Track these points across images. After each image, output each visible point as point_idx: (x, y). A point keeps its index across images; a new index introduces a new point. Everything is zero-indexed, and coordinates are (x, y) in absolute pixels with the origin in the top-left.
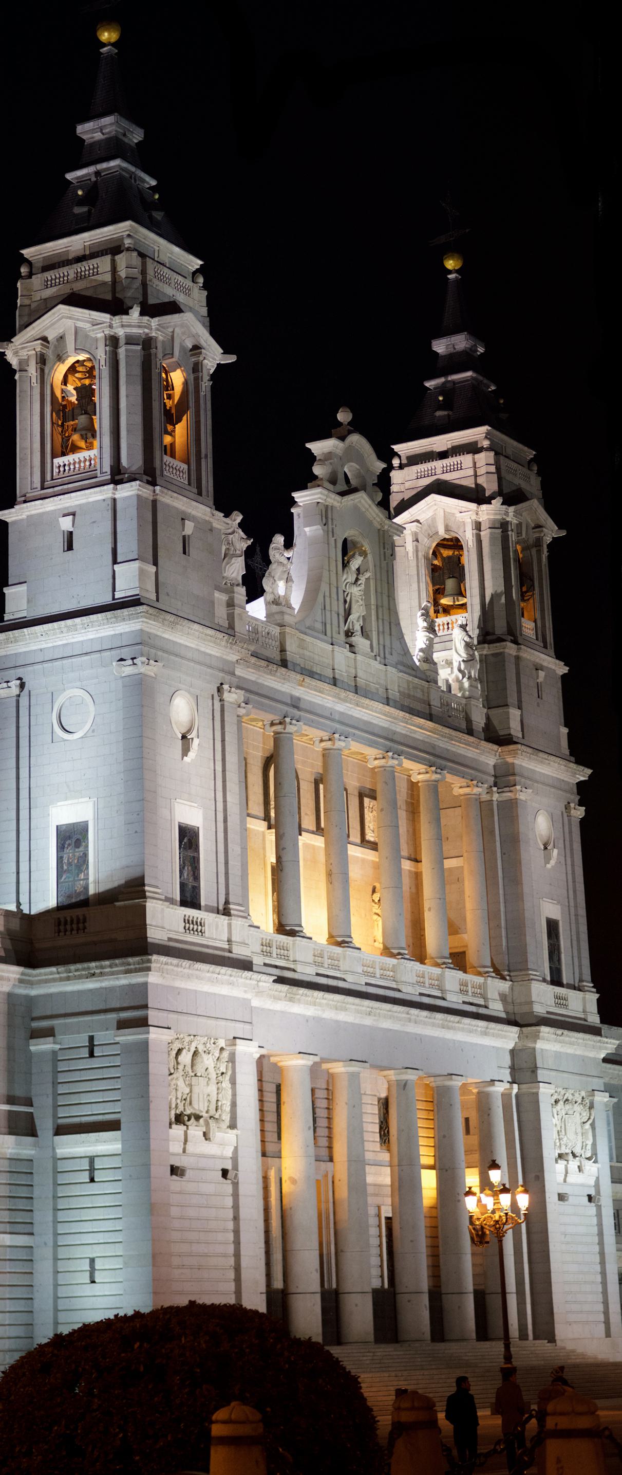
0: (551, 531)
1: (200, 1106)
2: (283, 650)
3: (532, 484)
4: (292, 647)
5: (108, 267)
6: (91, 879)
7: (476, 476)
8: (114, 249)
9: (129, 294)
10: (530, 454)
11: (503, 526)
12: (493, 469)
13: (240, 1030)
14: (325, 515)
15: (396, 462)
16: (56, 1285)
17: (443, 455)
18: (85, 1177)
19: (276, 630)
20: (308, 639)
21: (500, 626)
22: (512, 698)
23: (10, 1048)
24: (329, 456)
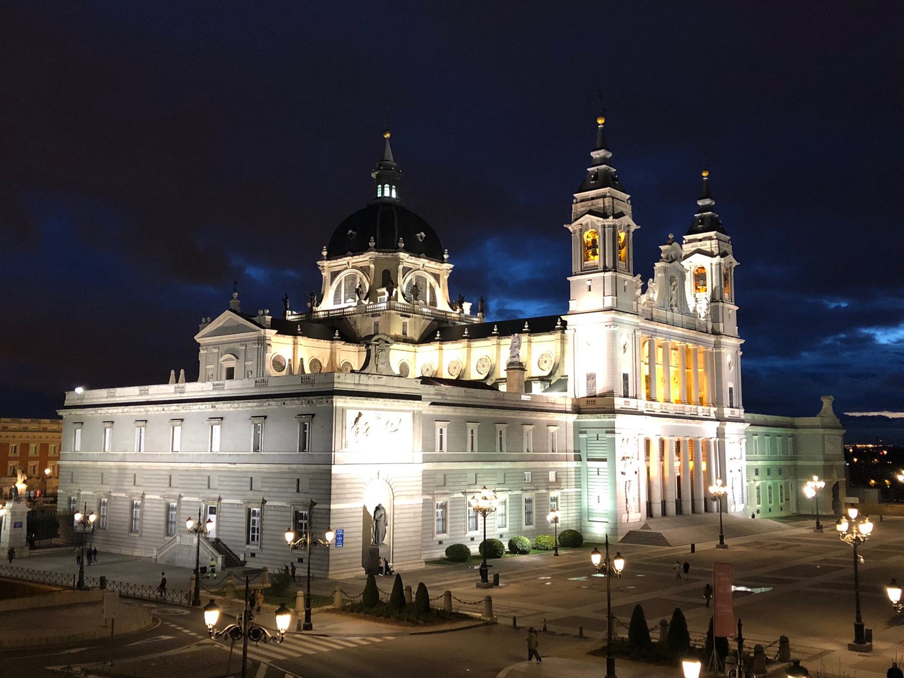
0: (735, 263)
2: (652, 315)
3: (729, 248)
4: (654, 314)
5: (602, 202)
8: (604, 196)
9: (609, 211)
10: (729, 238)
11: (720, 264)
12: (717, 245)
14: (665, 270)
15: (684, 242)
17: (700, 240)
18: (596, 473)
19: (650, 309)
20: (660, 310)
22: (721, 320)
23: (574, 437)
24: (666, 250)
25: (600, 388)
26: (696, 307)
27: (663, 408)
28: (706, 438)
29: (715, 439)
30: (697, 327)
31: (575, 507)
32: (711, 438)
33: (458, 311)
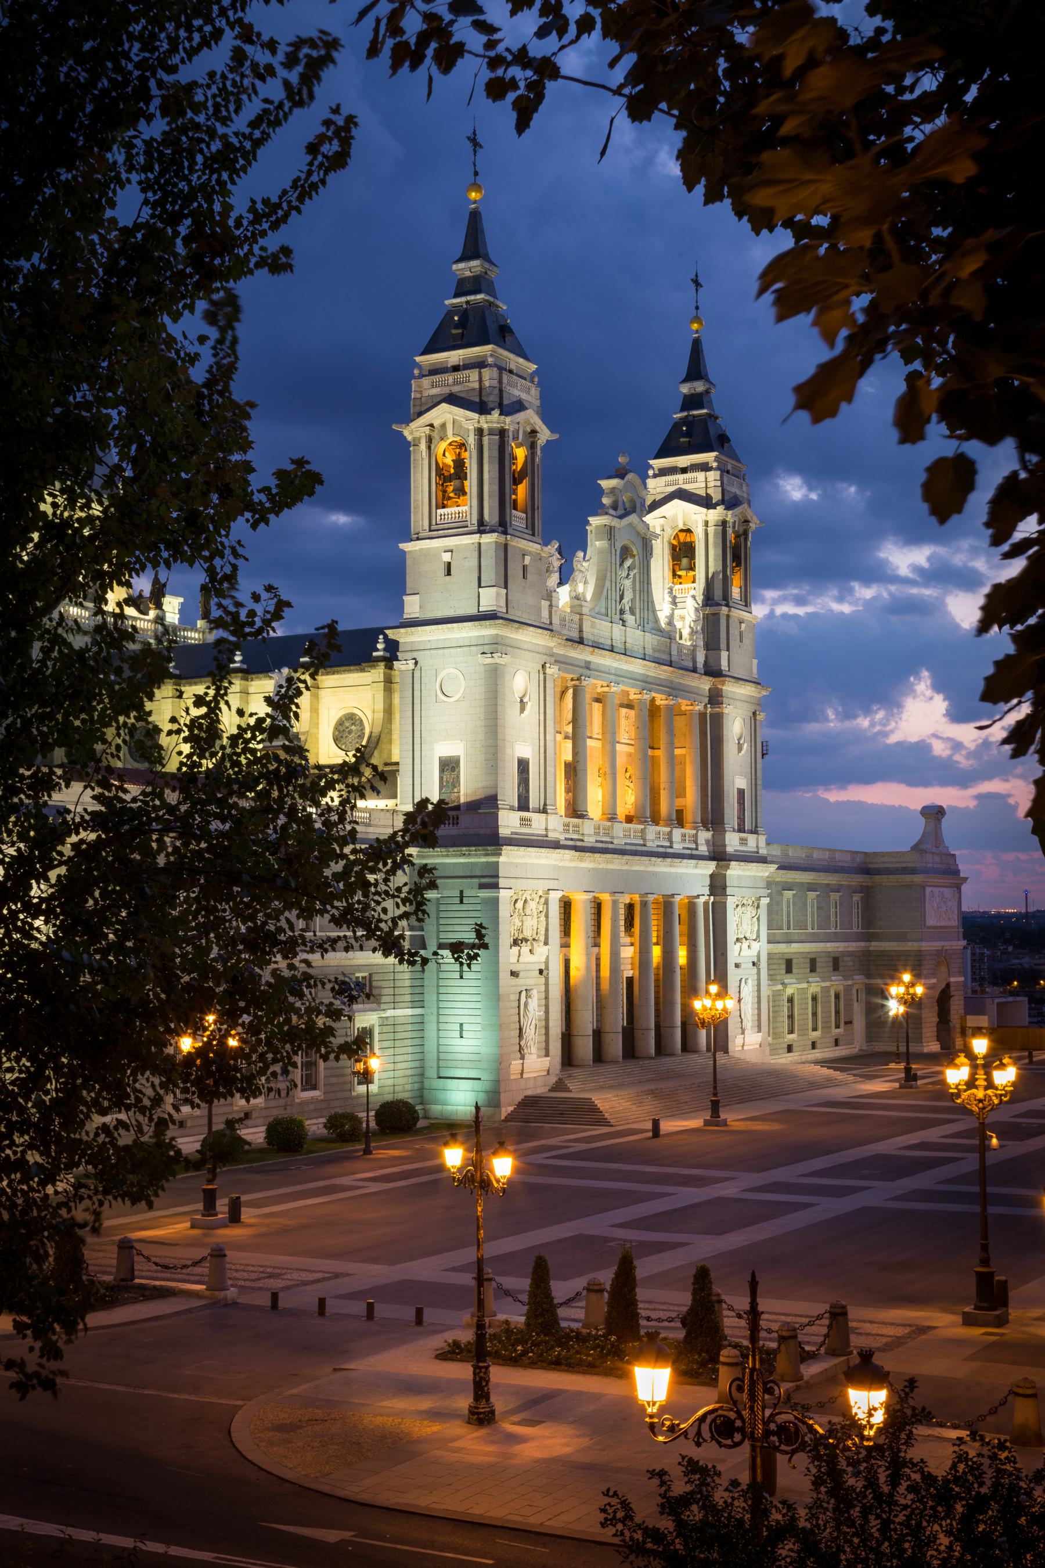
1: (528, 933)
2: (581, 631)
5: (477, 379)
6: (462, 792)
7: (706, 487)
8: (480, 364)
11: (724, 523)
12: (719, 483)
13: (552, 884)
14: (610, 533)
15: (651, 472)
16: (438, 1038)
17: (684, 470)
21: (718, 594)
22: (723, 645)
24: (613, 490)
25: (467, 790)
26: (672, 615)
27: (602, 831)
28: (688, 897)
29: (702, 899)
30: (673, 659)
31: (410, 1050)
32: (698, 896)
33: (152, 614)
